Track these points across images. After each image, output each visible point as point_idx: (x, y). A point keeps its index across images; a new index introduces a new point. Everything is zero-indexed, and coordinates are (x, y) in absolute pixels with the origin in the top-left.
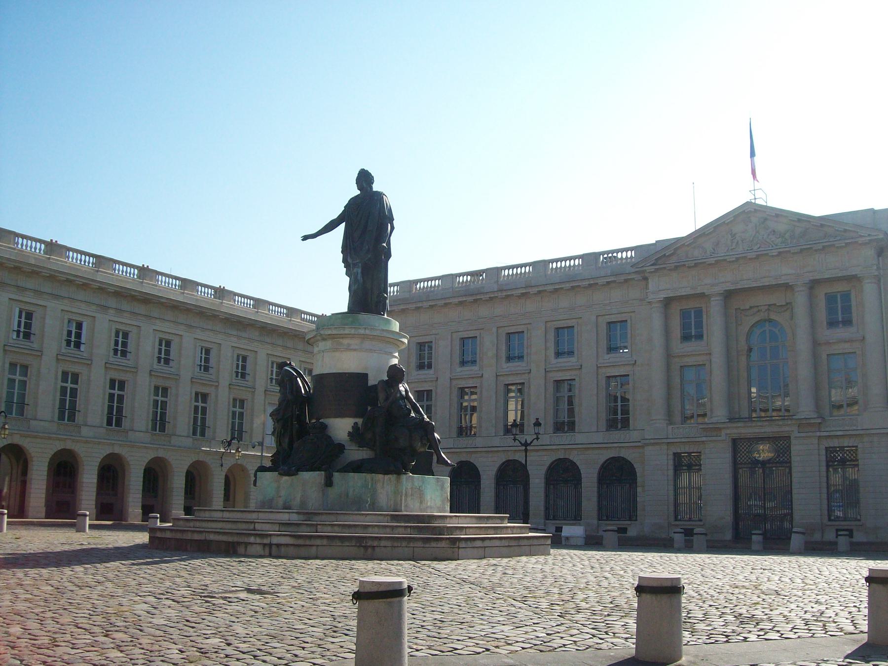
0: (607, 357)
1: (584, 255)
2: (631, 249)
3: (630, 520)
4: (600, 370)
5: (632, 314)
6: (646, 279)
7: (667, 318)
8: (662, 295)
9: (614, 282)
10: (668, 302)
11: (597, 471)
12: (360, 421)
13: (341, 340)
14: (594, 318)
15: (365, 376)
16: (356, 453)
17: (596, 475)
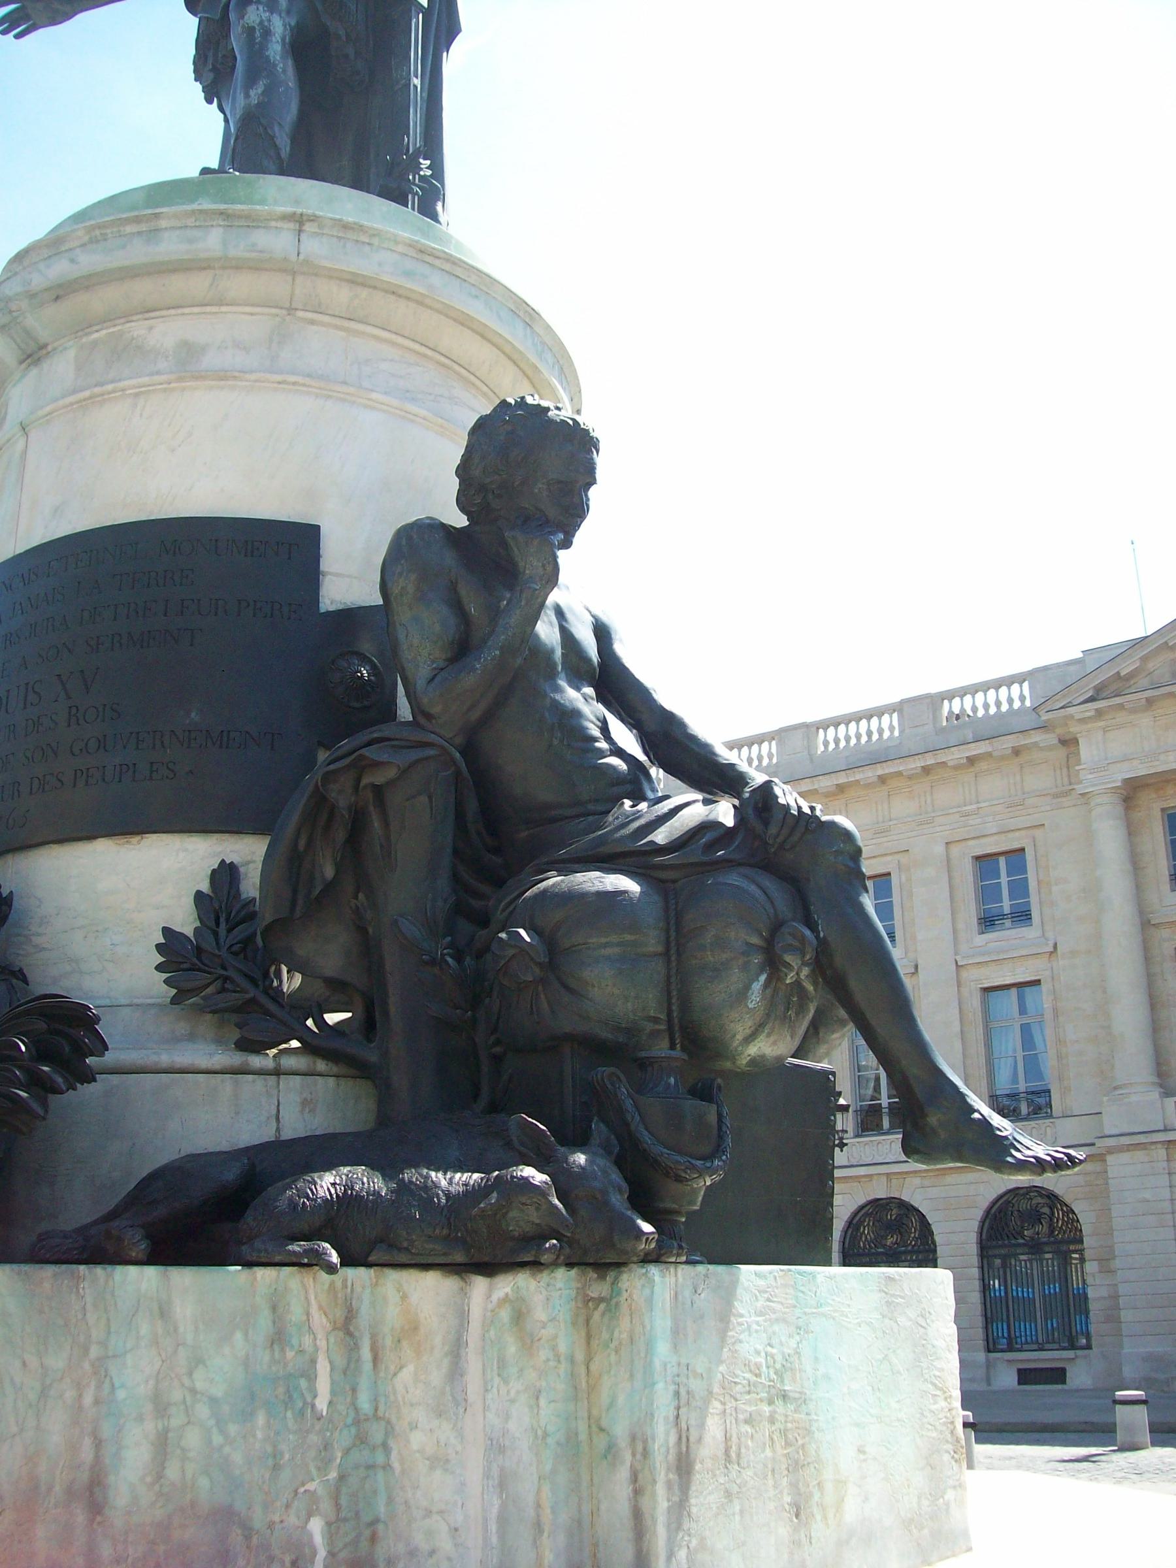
0: (980, 940)
1: (902, 702)
2: (1019, 679)
3: (1073, 1346)
4: (964, 974)
5: (1038, 833)
6: (1069, 743)
7: (1132, 831)
8: (1120, 774)
9: (988, 755)
10: (1131, 793)
11: (975, 1225)
12: (249, 852)
13: (137, 329)
14: (940, 849)
15: (295, 545)
16: (219, 1101)
17: (973, 1238)
